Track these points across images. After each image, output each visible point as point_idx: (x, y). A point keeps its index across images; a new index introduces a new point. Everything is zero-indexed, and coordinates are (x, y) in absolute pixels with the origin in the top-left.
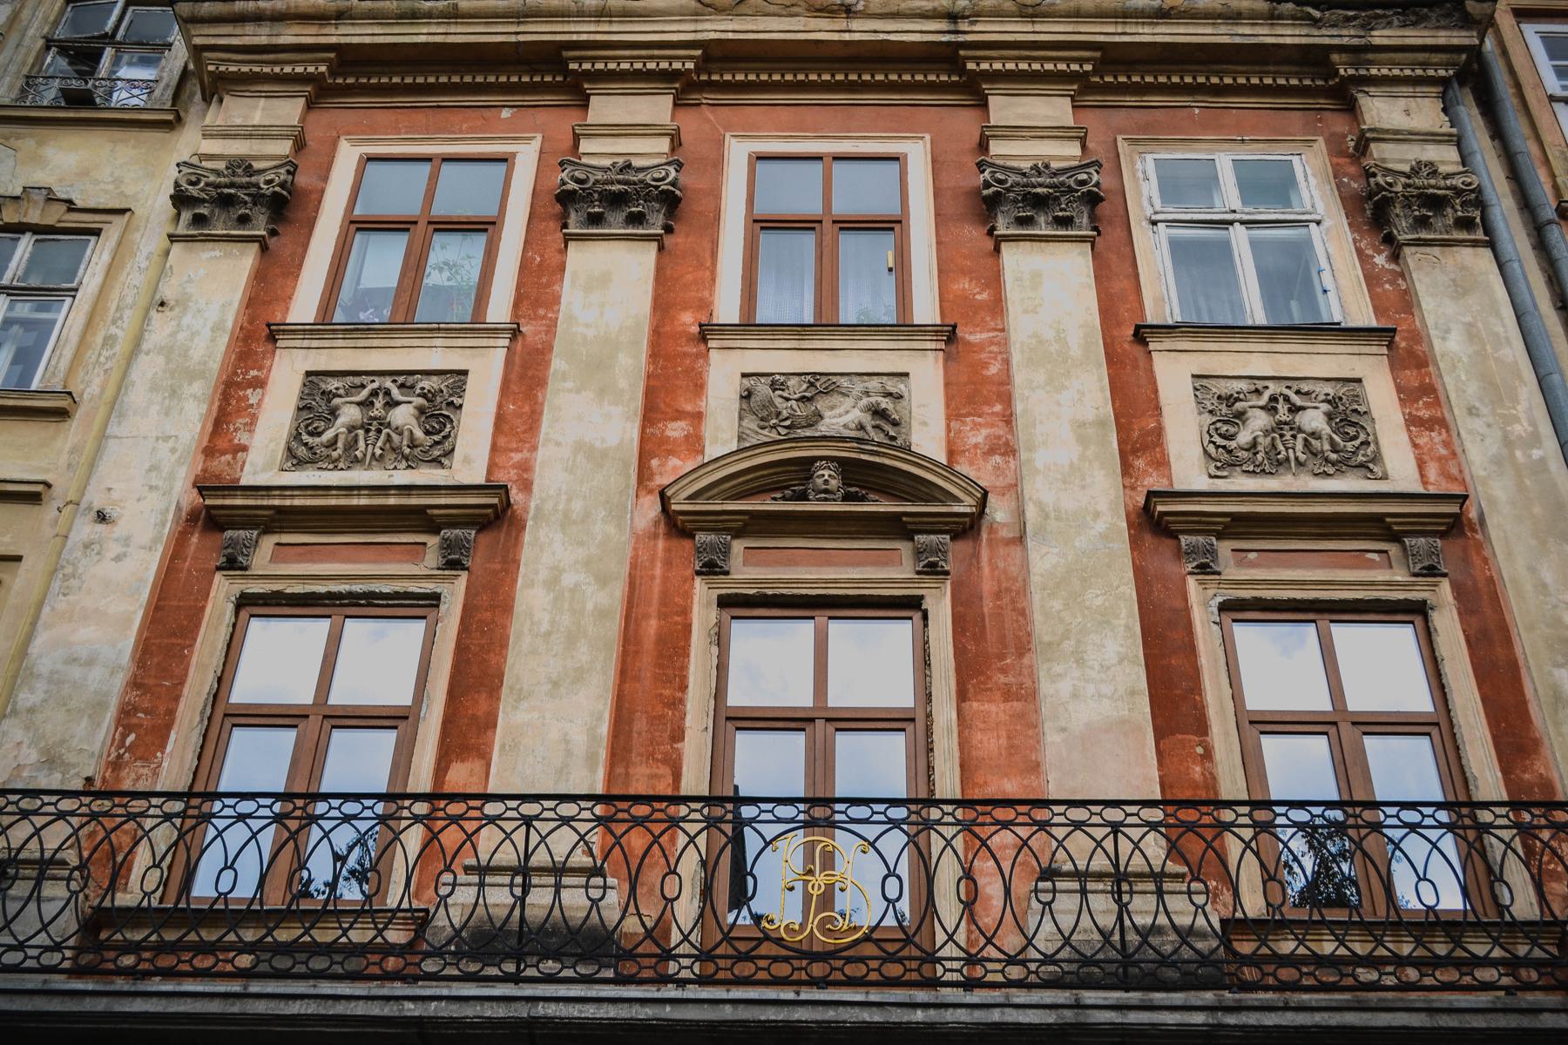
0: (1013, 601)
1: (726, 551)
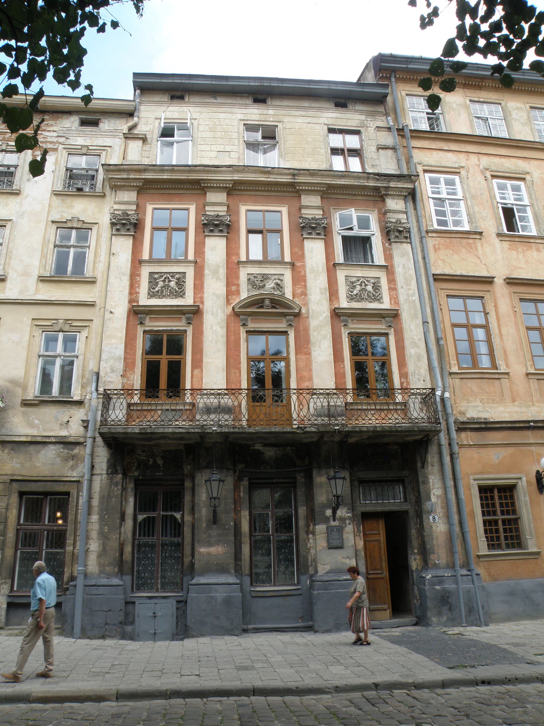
0: (307, 332)
1: (247, 320)
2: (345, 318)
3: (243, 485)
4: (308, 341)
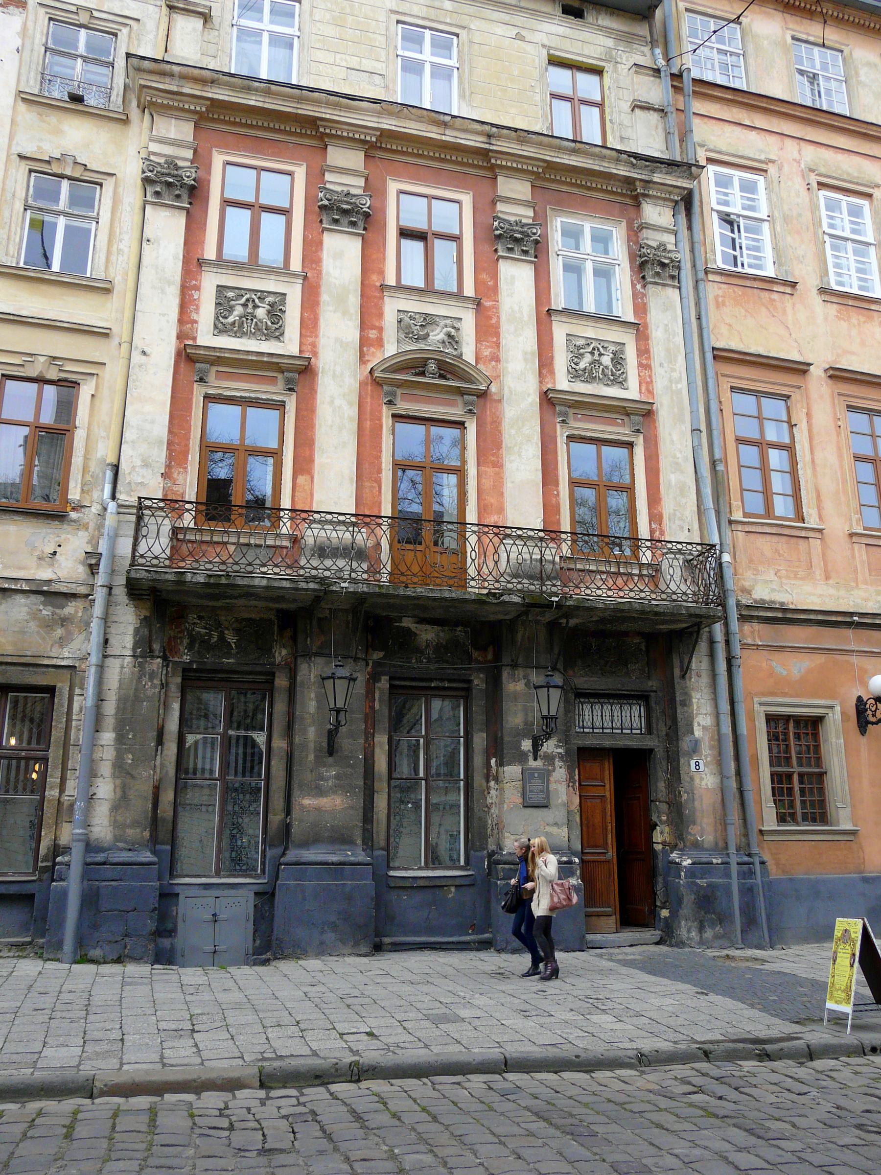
2: (563, 408)
3: (380, 689)
4: (498, 444)
